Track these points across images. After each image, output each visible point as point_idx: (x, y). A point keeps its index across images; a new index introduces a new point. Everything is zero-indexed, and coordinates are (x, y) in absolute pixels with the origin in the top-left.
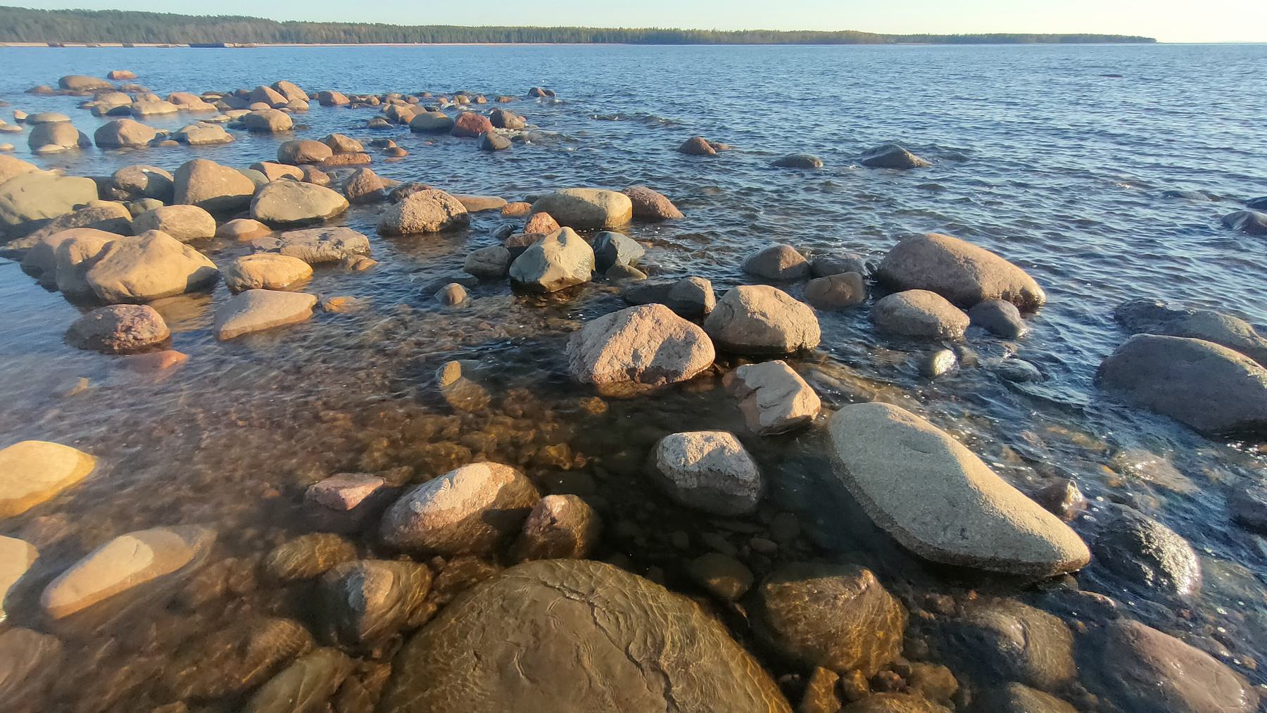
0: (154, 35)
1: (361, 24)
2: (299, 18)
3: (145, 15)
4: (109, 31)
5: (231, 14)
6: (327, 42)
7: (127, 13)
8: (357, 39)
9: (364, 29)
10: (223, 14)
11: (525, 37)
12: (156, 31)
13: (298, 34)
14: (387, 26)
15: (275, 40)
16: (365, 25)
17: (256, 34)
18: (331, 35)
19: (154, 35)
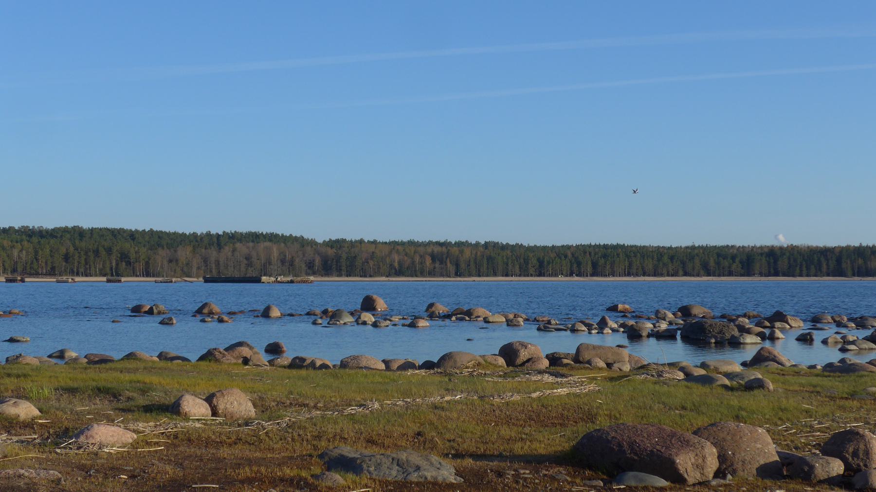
0: (129, 263)
1: (459, 244)
2: (351, 235)
3: (116, 234)
4: (67, 258)
5: (243, 227)
6: (399, 273)
7: (92, 231)
8: (451, 268)
9: (467, 253)
10: (230, 229)
11: (783, 264)
12: (133, 256)
13: (352, 259)
14: (505, 247)
15: (311, 268)
16: (466, 244)
17: (283, 262)
18: (408, 261)
19: (129, 263)
